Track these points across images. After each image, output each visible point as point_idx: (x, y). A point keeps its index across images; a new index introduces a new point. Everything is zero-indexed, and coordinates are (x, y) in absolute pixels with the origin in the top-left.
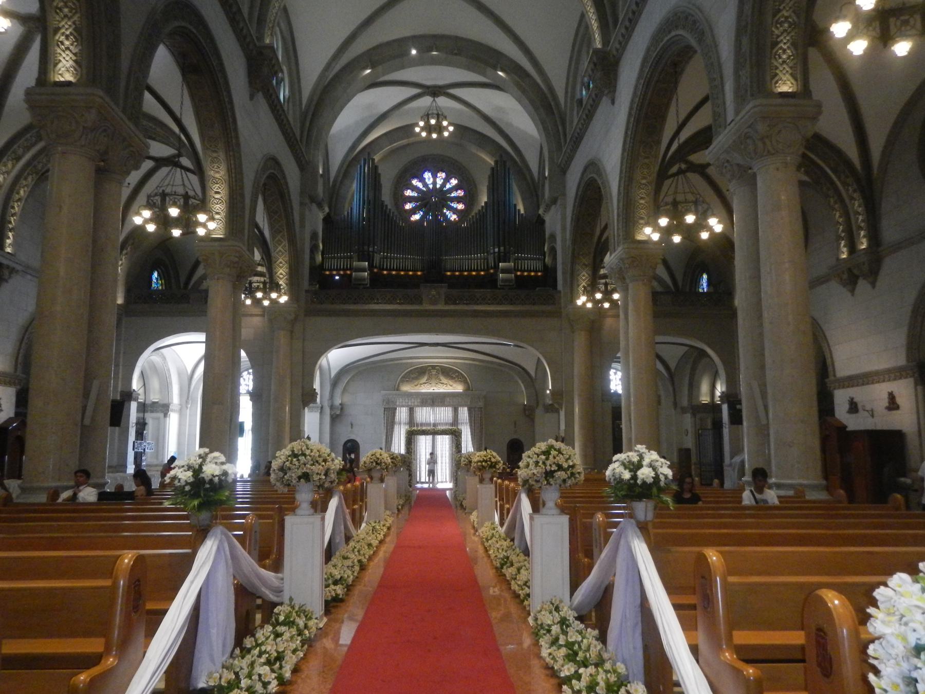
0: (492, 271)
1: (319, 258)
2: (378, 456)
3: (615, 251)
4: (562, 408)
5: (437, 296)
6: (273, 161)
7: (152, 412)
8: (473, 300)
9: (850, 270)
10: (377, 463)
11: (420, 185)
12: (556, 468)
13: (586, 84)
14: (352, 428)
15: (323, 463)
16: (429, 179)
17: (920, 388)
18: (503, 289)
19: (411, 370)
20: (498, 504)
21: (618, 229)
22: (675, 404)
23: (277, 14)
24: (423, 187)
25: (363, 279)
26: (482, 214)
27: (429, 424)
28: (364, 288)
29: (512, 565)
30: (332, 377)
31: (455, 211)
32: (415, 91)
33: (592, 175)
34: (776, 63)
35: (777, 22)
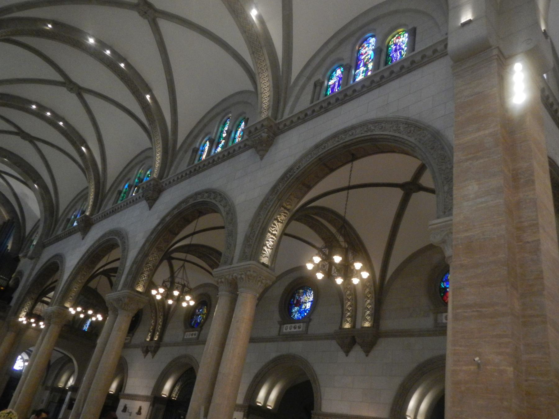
9: (147, 347)
17: (151, 407)
22: (44, 383)
34: (140, 280)
35: (146, 267)
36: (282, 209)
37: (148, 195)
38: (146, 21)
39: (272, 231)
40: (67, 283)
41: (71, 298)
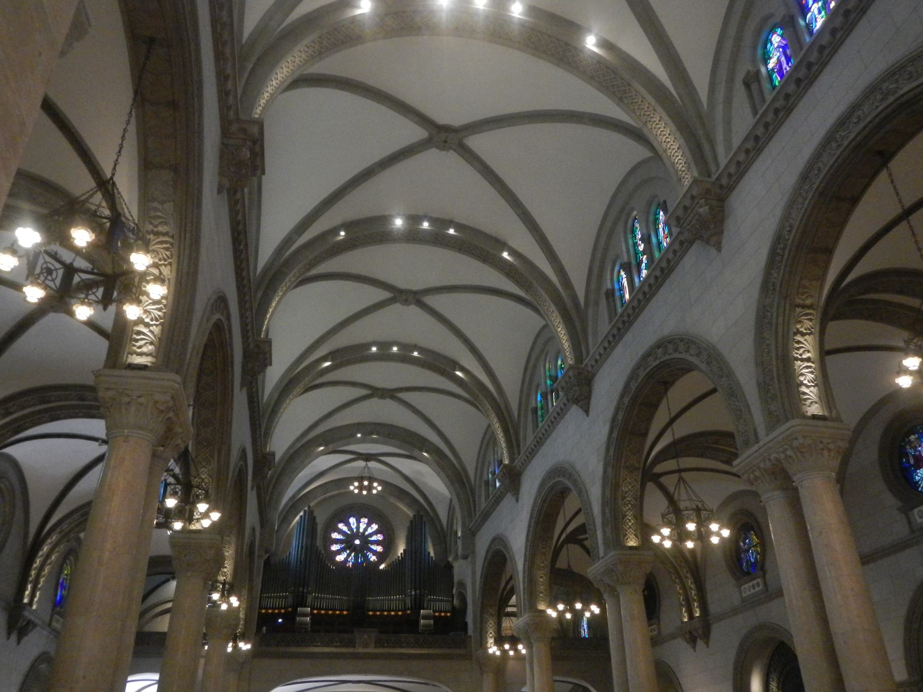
0: (409, 612)
5: (368, 640)
8: (399, 644)
9: (690, 632)
11: (345, 529)
16: (354, 524)
21: (524, 599)
25: (305, 624)
26: (401, 562)
33: (500, 547)
36: (798, 310)
37: (574, 395)
38: (452, 152)
39: (801, 355)
40: (526, 574)
41: (541, 595)
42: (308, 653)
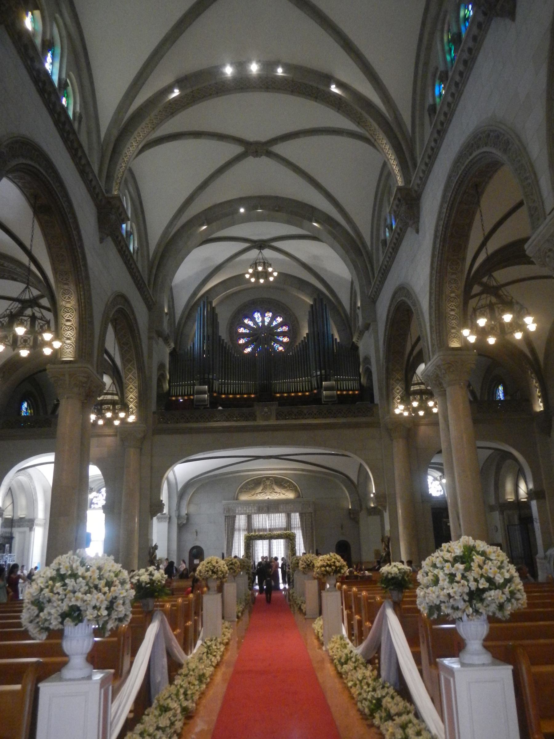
0: (315, 391)
1: (166, 386)
2: (214, 564)
3: (430, 360)
4: (386, 512)
6: (121, 298)
7: (19, 526)
8: (300, 415)
10: (213, 572)
11: (251, 323)
12: (487, 585)
13: (389, 226)
14: (197, 535)
15: (106, 589)
16: (258, 319)
18: (327, 404)
19: (248, 482)
20: (345, 612)
23: (123, 172)
24: (254, 325)
25: (204, 400)
26: (305, 345)
27: (265, 530)
28: (204, 408)
29: (390, 717)
30: (179, 489)
31: (281, 343)
32: (246, 245)
42: (205, 428)
